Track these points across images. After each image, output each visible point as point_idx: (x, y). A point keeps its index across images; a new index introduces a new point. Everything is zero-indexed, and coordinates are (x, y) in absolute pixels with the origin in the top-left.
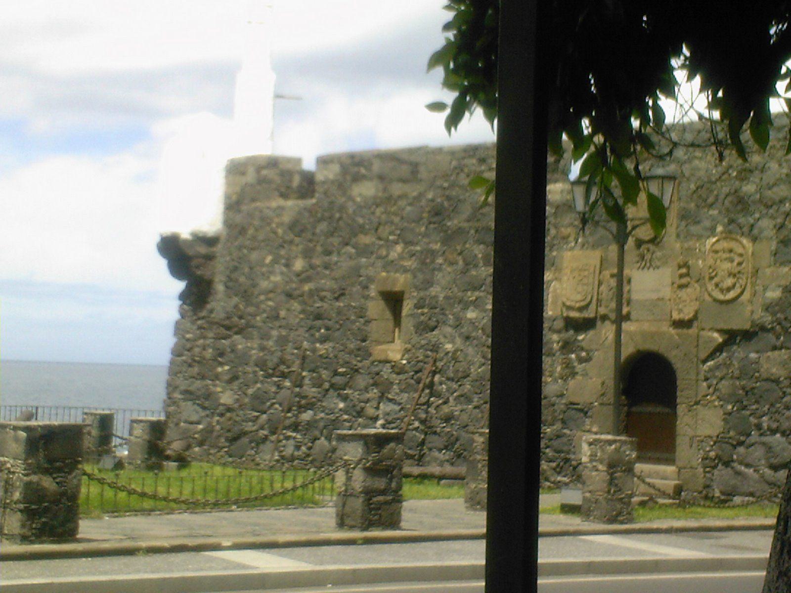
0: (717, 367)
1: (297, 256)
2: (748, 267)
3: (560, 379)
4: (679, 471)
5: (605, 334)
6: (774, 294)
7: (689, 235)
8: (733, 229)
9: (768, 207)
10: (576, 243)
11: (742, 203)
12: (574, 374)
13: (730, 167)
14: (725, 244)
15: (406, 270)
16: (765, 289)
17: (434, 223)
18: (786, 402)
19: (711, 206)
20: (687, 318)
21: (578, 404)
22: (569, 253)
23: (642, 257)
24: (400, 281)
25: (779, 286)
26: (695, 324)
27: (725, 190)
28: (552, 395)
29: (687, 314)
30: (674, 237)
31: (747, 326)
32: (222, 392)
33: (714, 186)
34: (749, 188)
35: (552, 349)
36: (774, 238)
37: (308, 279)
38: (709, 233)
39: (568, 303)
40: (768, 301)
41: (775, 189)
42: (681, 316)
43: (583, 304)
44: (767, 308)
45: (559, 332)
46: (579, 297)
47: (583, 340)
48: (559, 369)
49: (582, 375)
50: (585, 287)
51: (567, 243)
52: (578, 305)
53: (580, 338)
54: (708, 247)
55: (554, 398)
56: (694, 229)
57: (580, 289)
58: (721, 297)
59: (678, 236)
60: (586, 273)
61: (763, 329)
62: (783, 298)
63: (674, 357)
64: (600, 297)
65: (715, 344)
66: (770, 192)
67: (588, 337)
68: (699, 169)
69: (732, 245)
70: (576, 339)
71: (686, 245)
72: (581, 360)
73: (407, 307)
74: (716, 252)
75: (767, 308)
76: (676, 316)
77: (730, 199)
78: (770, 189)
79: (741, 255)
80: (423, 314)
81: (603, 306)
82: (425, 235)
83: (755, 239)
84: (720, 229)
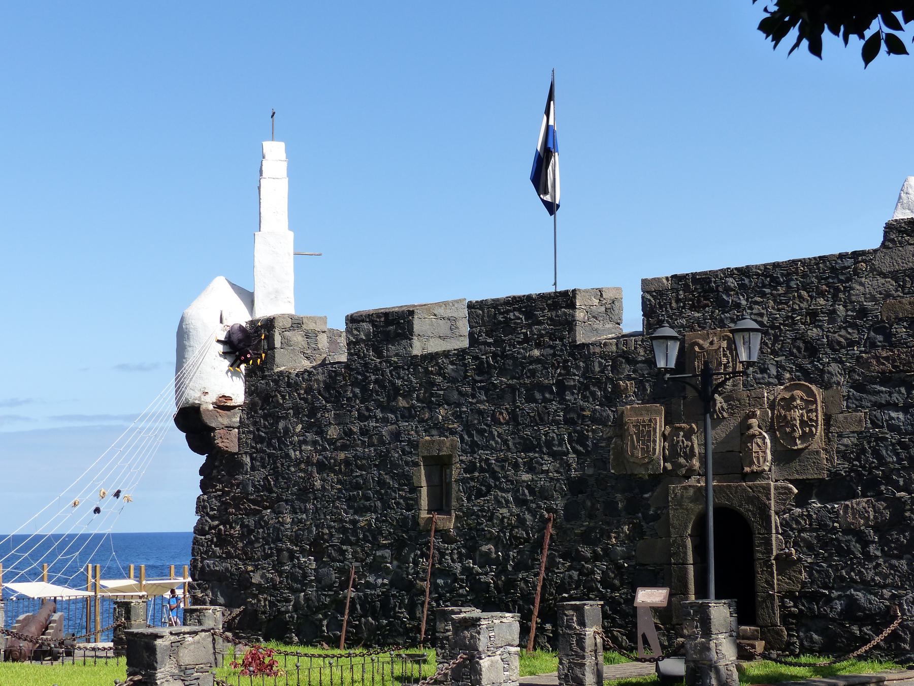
1: (330, 424)
15: (453, 432)
16: (840, 436)
17: (481, 382)
24: (448, 444)
25: (853, 432)
31: (825, 475)
32: (251, 571)
37: (344, 448)
40: (843, 448)
47: (650, 496)
53: (646, 496)
67: (655, 493)
73: (456, 472)
75: (843, 455)
80: (472, 479)
82: (473, 396)
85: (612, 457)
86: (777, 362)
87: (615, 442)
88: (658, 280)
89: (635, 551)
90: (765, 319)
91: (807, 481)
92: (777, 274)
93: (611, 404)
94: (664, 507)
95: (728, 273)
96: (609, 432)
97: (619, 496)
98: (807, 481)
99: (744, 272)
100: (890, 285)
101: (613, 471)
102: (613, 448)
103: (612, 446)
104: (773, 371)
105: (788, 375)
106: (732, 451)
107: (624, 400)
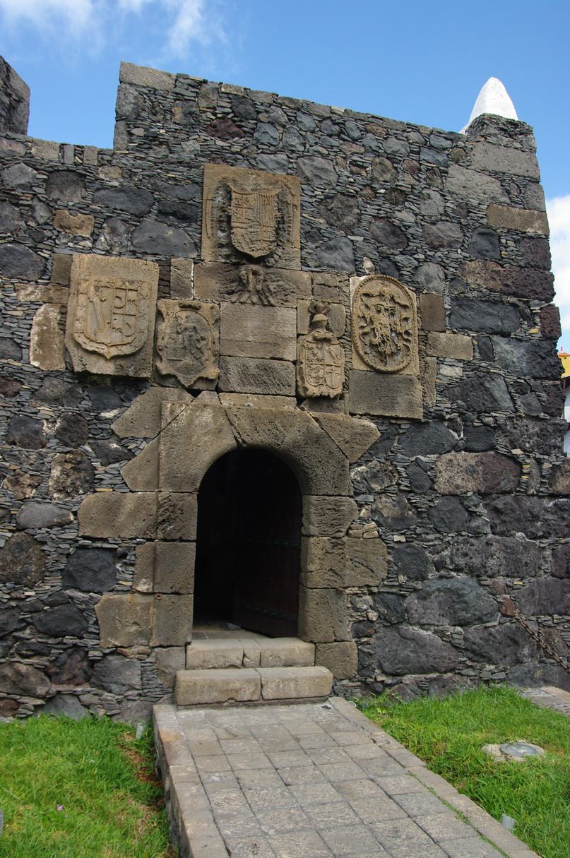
0: (375, 476)
2: (413, 326)
3: (59, 491)
4: (316, 648)
5: (172, 412)
6: (452, 372)
7: (321, 266)
8: (388, 269)
9: (434, 248)
10: (95, 241)
11: (398, 232)
12: (92, 483)
13: (373, 179)
14: (376, 287)
16: (441, 362)
18: (478, 527)
19: (349, 230)
20: (333, 393)
21: (105, 540)
22: (87, 257)
23: (242, 284)
25: (460, 361)
26: (338, 404)
27: (371, 210)
28: (39, 524)
29: (333, 383)
30: (297, 263)
31: (419, 414)
33: (352, 202)
34: (405, 216)
35: (37, 432)
36: (447, 292)
38: (351, 268)
39: (91, 347)
40: (445, 381)
41: (440, 225)
42: (324, 390)
43: (127, 350)
44: (444, 391)
45: (56, 401)
46: (116, 338)
48: (56, 472)
49: (113, 485)
50: (131, 321)
51: (75, 239)
52: (114, 352)
54: (352, 288)
55: (44, 530)
56: (328, 257)
57: (118, 321)
58: (379, 367)
59: (304, 263)
60: (132, 295)
61: (440, 418)
62: (465, 378)
63: (311, 458)
64: (160, 343)
65: (373, 439)
66: (433, 227)
67: (128, 413)
68: (325, 170)
69: (391, 289)
70: (97, 418)
71: (319, 278)
72: (110, 458)
74: (367, 295)
76: (313, 390)
77: (380, 224)
78: (434, 223)
79: (405, 307)
81: (164, 359)
83: (418, 291)
84: (368, 264)
85: (36, 338)
86: (352, 241)
87: (46, 313)
88: (152, 72)
89: (75, 513)
90: (333, 178)
91: (394, 422)
92: (351, 125)
93: (40, 246)
94: (145, 439)
95: (276, 101)
96: (32, 293)
97: (45, 410)
98: (394, 422)
99: (298, 108)
100: (495, 187)
101: (36, 364)
102: (39, 324)
103: (37, 319)
104: (348, 252)
105: (368, 264)
106: (281, 359)
107: (70, 244)
